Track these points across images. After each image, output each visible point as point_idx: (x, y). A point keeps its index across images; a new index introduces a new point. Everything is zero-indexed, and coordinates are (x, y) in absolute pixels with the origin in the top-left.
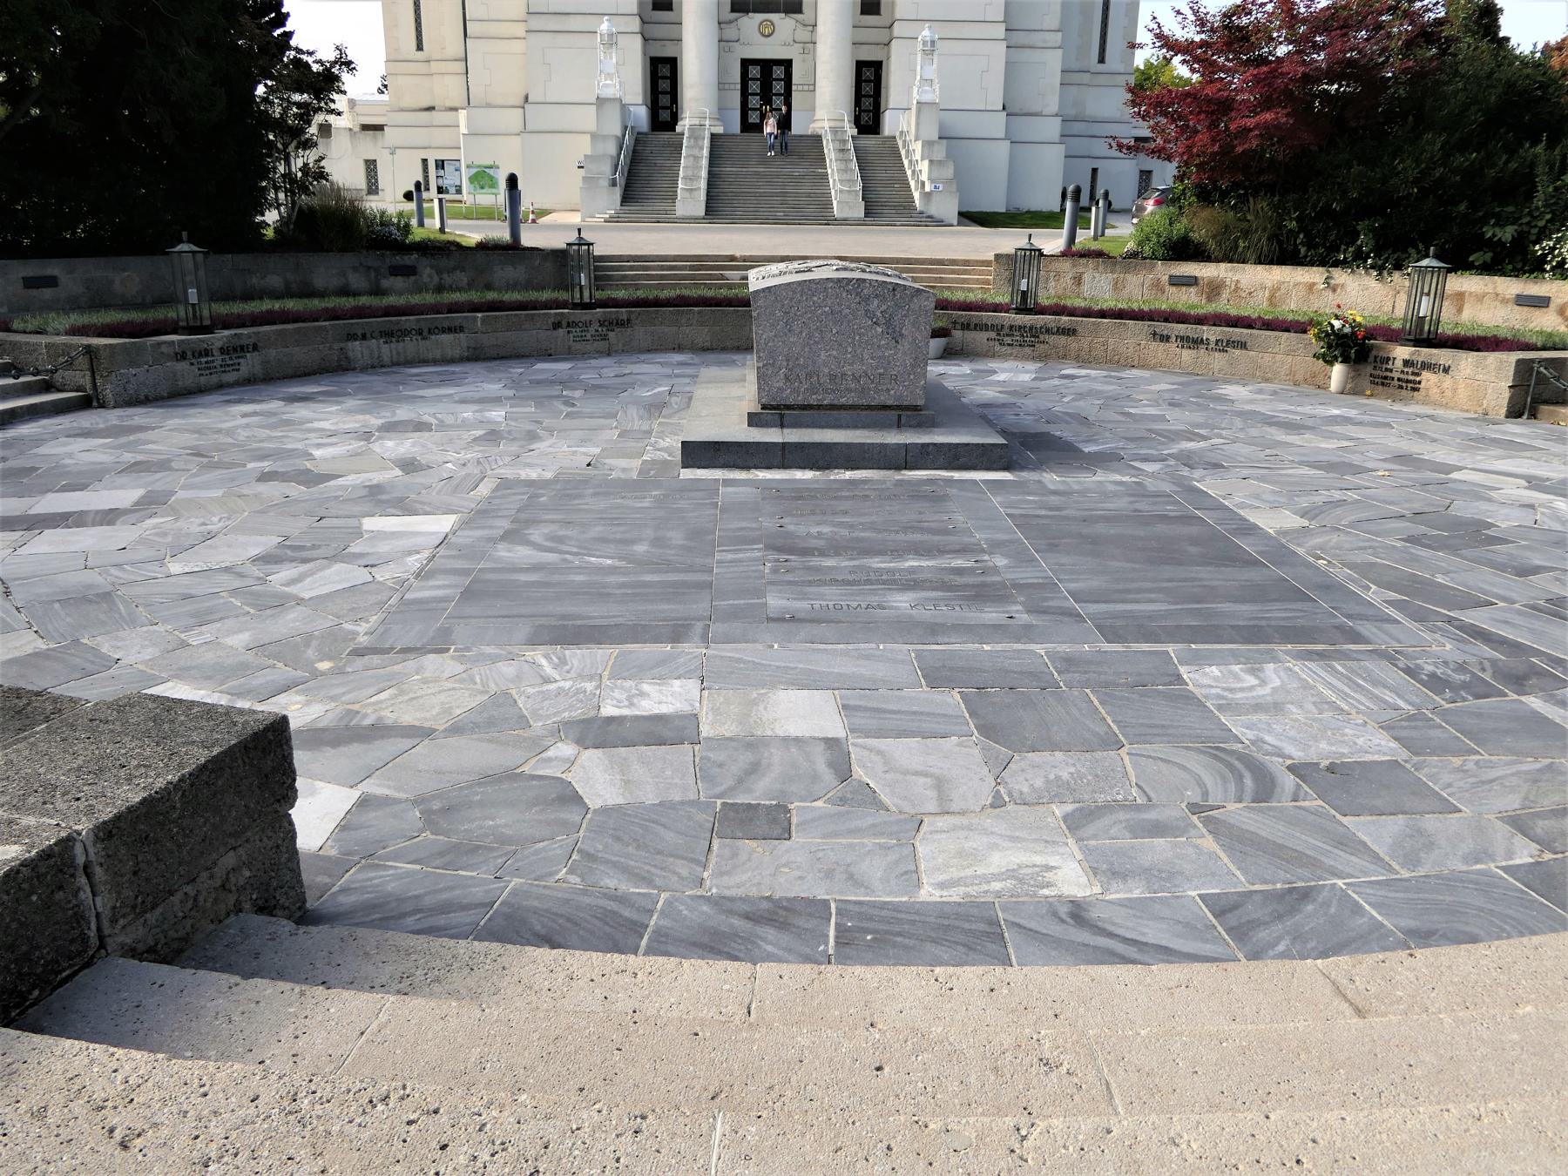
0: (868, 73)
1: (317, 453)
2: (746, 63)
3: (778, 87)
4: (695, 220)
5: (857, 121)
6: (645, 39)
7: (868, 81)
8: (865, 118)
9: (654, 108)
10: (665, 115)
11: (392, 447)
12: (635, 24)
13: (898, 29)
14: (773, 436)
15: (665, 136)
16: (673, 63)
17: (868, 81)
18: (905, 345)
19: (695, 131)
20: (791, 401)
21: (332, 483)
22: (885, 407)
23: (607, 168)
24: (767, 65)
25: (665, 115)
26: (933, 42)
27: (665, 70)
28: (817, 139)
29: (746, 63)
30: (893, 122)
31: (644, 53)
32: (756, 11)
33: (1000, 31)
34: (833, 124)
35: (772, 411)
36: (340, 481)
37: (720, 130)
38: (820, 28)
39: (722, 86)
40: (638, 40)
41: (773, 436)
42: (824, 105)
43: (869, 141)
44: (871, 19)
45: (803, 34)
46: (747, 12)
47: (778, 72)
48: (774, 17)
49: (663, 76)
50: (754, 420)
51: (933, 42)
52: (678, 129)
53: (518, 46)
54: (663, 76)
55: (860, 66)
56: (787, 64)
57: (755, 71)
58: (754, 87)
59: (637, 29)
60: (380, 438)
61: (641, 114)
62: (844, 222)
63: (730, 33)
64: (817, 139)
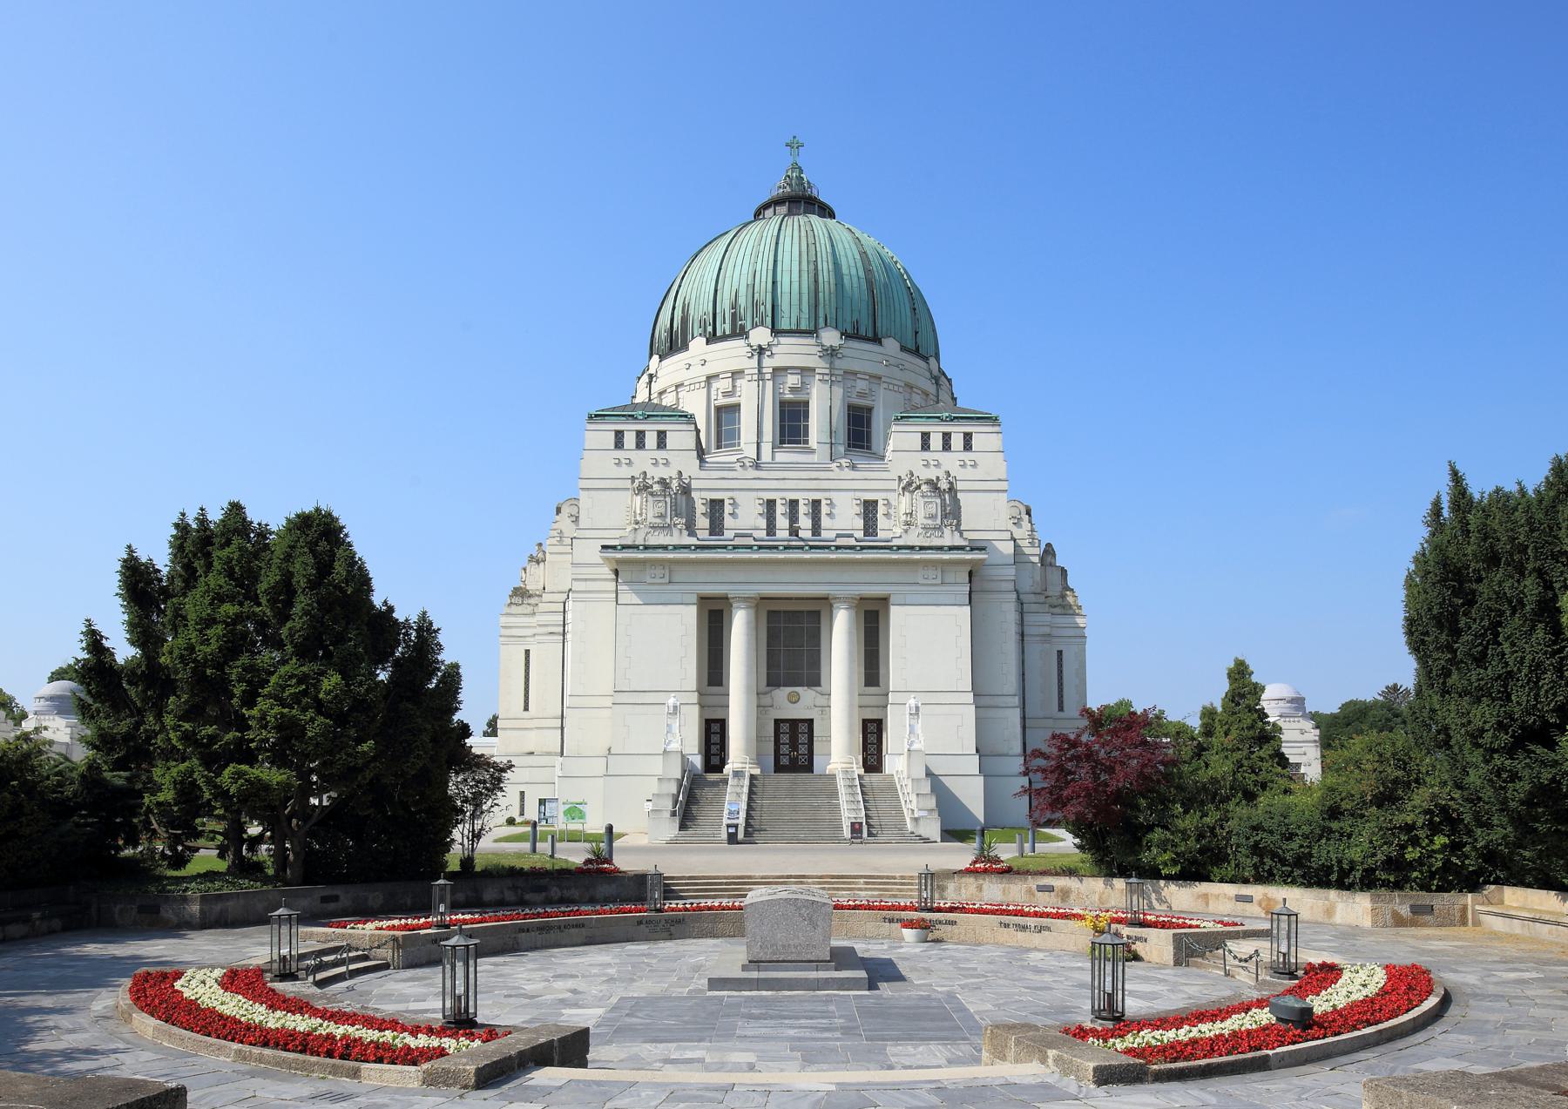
2: (777, 722)
3: (803, 739)
7: (872, 734)
10: (715, 761)
12: (694, 698)
14: (754, 975)
15: (712, 777)
16: (723, 723)
17: (872, 734)
18: (819, 930)
19: (738, 774)
23: (669, 805)
24: (794, 723)
25: (715, 761)
26: (917, 708)
27: (715, 728)
29: (777, 722)
30: (894, 764)
31: (701, 716)
32: (785, 685)
33: (970, 697)
35: (755, 963)
37: (757, 771)
39: (760, 738)
40: (696, 708)
41: (754, 975)
42: (838, 752)
43: (874, 778)
45: (821, 701)
46: (778, 685)
47: (803, 728)
48: (798, 689)
49: (714, 734)
50: (744, 968)
51: (917, 708)
52: (725, 771)
53: (607, 713)
54: (714, 734)
55: (865, 722)
56: (810, 722)
57: (785, 728)
58: (785, 739)
61: (698, 761)
63: (766, 700)
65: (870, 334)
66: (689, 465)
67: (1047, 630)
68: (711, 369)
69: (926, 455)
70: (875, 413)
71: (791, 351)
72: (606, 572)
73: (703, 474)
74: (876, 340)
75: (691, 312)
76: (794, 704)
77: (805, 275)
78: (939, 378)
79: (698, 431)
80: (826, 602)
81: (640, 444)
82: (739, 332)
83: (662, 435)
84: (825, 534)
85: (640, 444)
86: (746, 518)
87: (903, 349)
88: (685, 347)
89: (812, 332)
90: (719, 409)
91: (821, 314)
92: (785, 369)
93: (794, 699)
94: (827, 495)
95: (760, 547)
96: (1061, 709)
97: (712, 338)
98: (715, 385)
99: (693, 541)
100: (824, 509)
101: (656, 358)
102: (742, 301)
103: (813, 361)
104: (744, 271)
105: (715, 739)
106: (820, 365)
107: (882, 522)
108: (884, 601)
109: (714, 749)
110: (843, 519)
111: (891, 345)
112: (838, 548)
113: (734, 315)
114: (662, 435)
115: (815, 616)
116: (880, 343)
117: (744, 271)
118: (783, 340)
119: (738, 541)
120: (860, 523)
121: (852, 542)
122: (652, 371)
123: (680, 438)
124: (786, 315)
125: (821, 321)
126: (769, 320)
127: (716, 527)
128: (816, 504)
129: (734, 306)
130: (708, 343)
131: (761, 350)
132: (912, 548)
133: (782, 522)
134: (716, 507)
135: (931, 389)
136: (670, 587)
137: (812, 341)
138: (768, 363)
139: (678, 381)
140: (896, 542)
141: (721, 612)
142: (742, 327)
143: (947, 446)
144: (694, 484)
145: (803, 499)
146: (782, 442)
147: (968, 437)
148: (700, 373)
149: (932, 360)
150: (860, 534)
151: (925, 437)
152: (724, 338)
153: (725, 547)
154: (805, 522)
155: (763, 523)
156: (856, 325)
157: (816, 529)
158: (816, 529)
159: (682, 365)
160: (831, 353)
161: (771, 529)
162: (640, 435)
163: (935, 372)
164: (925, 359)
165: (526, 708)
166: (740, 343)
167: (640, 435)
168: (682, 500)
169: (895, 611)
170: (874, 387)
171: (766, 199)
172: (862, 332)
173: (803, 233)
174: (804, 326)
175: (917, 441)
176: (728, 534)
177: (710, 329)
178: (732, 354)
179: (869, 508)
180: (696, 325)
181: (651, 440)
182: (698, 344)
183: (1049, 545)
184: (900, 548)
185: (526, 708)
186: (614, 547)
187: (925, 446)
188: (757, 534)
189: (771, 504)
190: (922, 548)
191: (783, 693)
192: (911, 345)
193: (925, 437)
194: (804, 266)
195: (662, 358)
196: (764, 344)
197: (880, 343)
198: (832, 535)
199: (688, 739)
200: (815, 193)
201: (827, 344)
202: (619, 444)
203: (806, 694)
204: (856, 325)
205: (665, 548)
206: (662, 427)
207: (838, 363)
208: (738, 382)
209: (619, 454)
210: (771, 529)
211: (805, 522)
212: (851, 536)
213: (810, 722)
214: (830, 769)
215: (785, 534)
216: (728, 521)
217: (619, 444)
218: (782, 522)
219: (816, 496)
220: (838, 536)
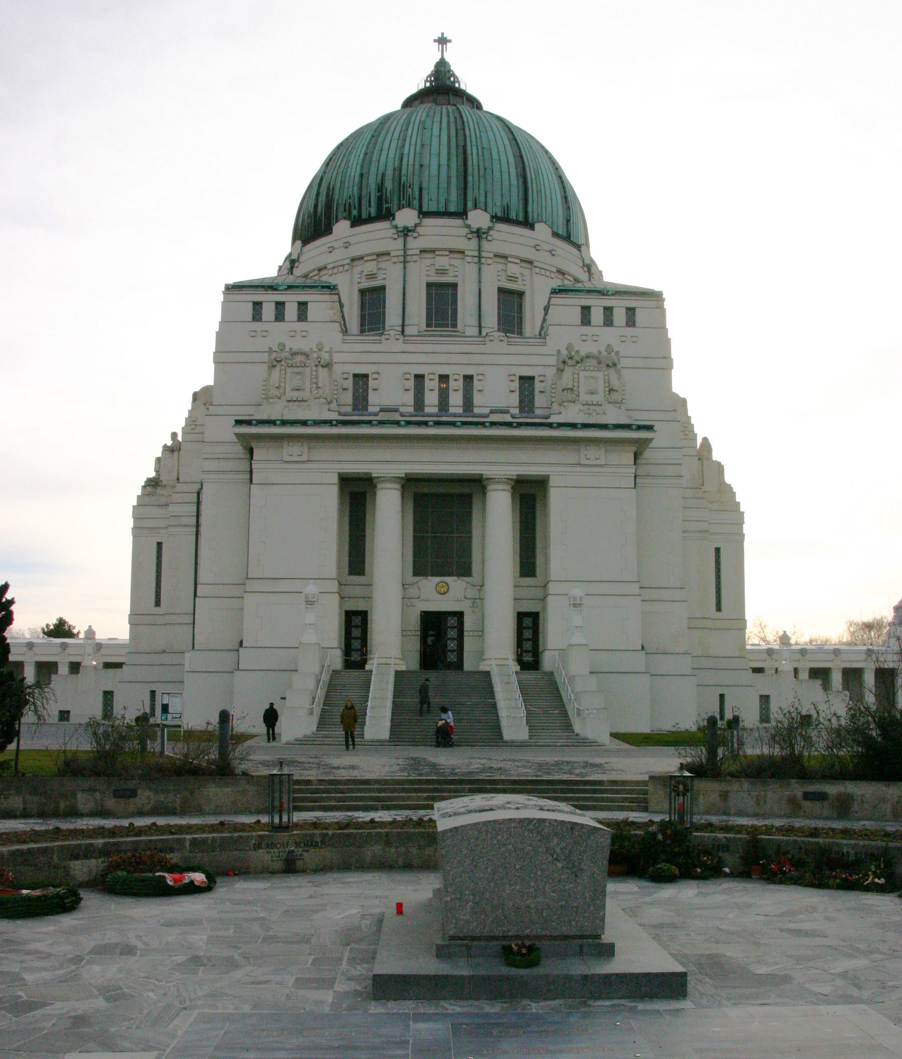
0: (527, 622)
1: (29, 977)
3: (452, 633)
4: (379, 743)
5: (519, 660)
6: (342, 598)
7: (529, 628)
8: (528, 658)
9: (348, 650)
10: (355, 657)
11: (98, 972)
12: (334, 586)
13: (552, 588)
15: (355, 673)
16: (364, 615)
17: (529, 628)
20: (478, 932)
21: (39, 1013)
22: (566, 937)
27: (357, 620)
28: (487, 674)
31: (341, 608)
34: (499, 662)
36: (48, 1010)
38: (487, 588)
39: (404, 633)
42: (492, 648)
44: (528, 581)
45: (472, 593)
46: (425, 575)
47: (452, 621)
48: (448, 579)
49: (356, 626)
52: (367, 667)
54: (356, 626)
55: (521, 616)
56: (460, 615)
59: (336, 590)
60: (89, 963)
62: (512, 744)
63: (413, 592)
64: (487, 674)
65: (521, 219)
66: (331, 336)
67: (704, 526)
68: (354, 252)
69: (585, 329)
70: (527, 298)
71: (440, 233)
72: (239, 449)
73: (346, 347)
74: (527, 223)
75: (336, 197)
76: (441, 594)
77: (454, 159)
78: (589, 267)
79: (342, 306)
80: (476, 485)
81: (280, 316)
82: (384, 214)
83: (303, 306)
84: (476, 411)
85: (280, 316)
86: (390, 393)
87: (555, 234)
88: (328, 231)
89: (462, 214)
90: (362, 292)
91: (470, 197)
92: (433, 251)
93: (443, 592)
94: (480, 369)
95: (408, 423)
96: (719, 609)
97: (357, 222)
98: (358, 269)
99: (334, 416)
100: (476, 385)
101: (299, 243)
102: (389, 184)
103: (461, 243)
104: (391, 155)
105: (356, 632)
106: (470, 246)
107: (540, 400)
108: (541, 483)
109: (356, 644)
110: (496, 394)
111: (542, 231)
112: (493, 424)
113: (380, 200)
114: (303, 306)
115: (466, 500)
116: (532, 227)
117: (391, 155)
118: (427, 221)
119: (383, 417)
120: (515, 399)
121: (507, 418)
122: (294, 257)
123: (320, 307)
124: (434, 197)
125: (470, 204)
126: (416, 203)
127: (361, 401)
128: (468, 379)
129: (381, 188)
130: (353, 225)
131: (406, 232)
132: (573, 426)
133: (431, 399)
134: (361, 379)
135: (583, 276)
136: (309, 466)
137: (459, 222)
138: (415, 244)
139: (321, 264)
140: (554, 419)
141: (364, 495)
142: (388, 209)
143: (608, 321)
144: (337, 357)
145: (457, 372)
146: (428, 325)
147: (631, 311)
148: (342, 255)
149: (583, 248)
150: (516, 411)
151: (586, 310)
152: (370, 220)
153: (369, 422)
154: (456, 400)
155: (410, 398)
156: (507, 209)
157: (468, 404)
158: (468, 404)
159: (325, 249)
160: (479, 234)
161: (419, 403)
162: (280, 305)
163: (587, 262)
164: (578, 247)
165: (158, 603)
166: (384, 225)
167: (280, 305)
168: (323, 373)
169: (554, 495)
170: (526, 272)
171: (414, 90)
172: (513, 215)
173: (452, 119)
174: (452, 208)
175: (576, 315)
176: (371, 409)
177: (355, 212)
178: (376, 236)
179: (526, 382)
180: (341, 208)
181: (291, 311)
182: (342, 227)
183: (705, 440)
184: (561, 425)
185: (158, 603)
186: (249, 423)
187: (586, 320)
188: (402, 409)
189: (419, 378)
190: (585, 426)
191: (429, 584)
192: (562, 231)
193: (586, 310)
194: (453, 151)
195: (305, 242)
196: (410, 224)
197: (532, 227)
198: (487, 411)
199: (332, 632)
200: (463, 87)
201: (475, 226)
202: (257, 316)
203: (456, 584)
204: (507, 209)
205: (304, 423)
206: (303, 298)
207: (485, 245)
208: (382, 265)
209: (257, 326)
210: (419, 403)
211: (456, 400)
212: (507, 412)
213: (460, 615)
214: (483, 667)
215: (435, 410)
216: (372, 398)
217: (257, 316)
218: (431, 399)
219: (469, 371)
220: (492, 412)
